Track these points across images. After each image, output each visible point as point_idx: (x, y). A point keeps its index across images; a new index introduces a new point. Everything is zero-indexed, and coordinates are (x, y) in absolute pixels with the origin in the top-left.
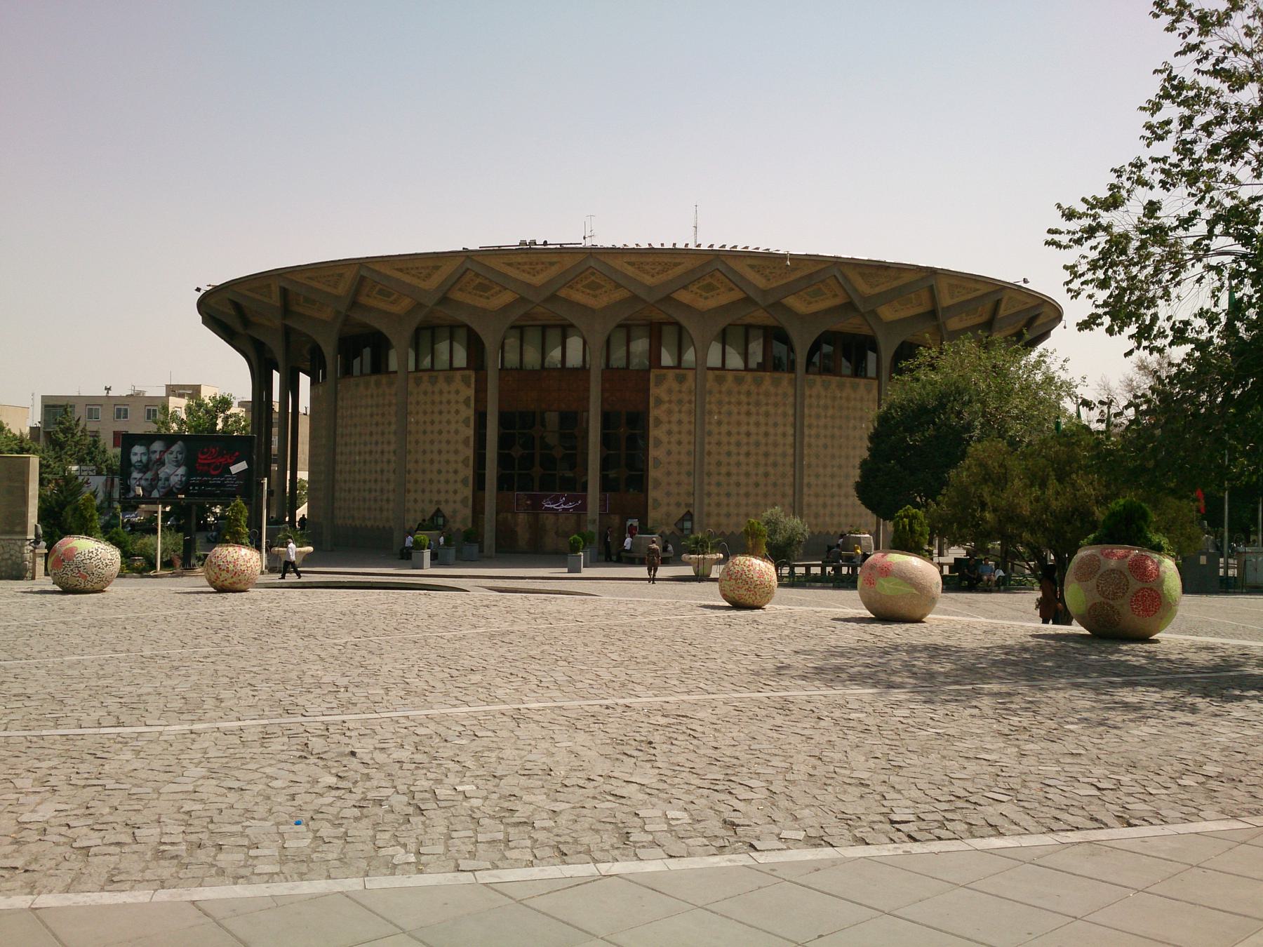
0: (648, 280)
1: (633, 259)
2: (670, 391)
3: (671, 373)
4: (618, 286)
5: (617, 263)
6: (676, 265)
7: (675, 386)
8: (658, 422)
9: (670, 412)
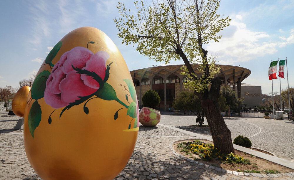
0: (172, 70)
1: (169, 67)
2: (178, 86)
3: (178, 84)
4: (167, 71)
5: (167, 68)
6: (175, 67)
7: (179, 85)
8: (176, 91)
9: (178, 89)
